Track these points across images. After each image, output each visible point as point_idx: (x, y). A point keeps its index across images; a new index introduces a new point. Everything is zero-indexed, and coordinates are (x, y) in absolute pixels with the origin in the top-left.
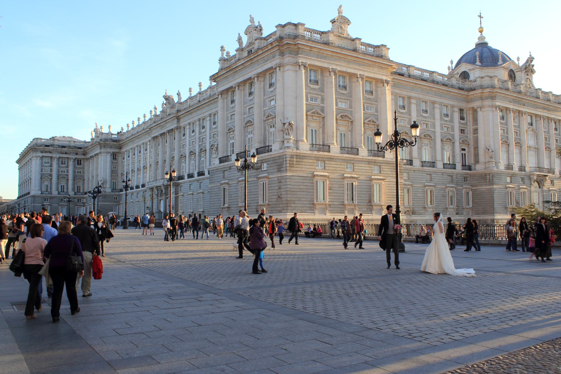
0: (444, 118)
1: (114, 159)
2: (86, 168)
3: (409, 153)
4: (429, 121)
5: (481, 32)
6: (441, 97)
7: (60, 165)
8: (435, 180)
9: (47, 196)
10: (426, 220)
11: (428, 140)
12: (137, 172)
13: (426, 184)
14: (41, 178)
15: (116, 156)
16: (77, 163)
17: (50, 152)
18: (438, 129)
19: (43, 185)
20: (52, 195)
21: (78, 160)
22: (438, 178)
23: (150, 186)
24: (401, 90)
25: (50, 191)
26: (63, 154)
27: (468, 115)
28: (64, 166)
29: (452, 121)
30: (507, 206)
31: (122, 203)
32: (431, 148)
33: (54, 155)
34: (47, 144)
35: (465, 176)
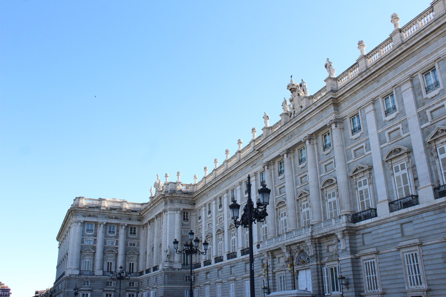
1: (184, 219)
2: (142, 238)
7: (108, 234)
9: (87, 278)
12: (228, 233)
14: (81, 252)
15: (187, 216)
16: (129, 232)
17: (94, 216)
19: (82, 261)
20: (94, 276)
21: (131, 228)
23: (273, 245)
25: (91, 270)
26: (112, 218)
28: (112, 235)
31: (199, 286)
33: (100, 221)
34: (92, 206)
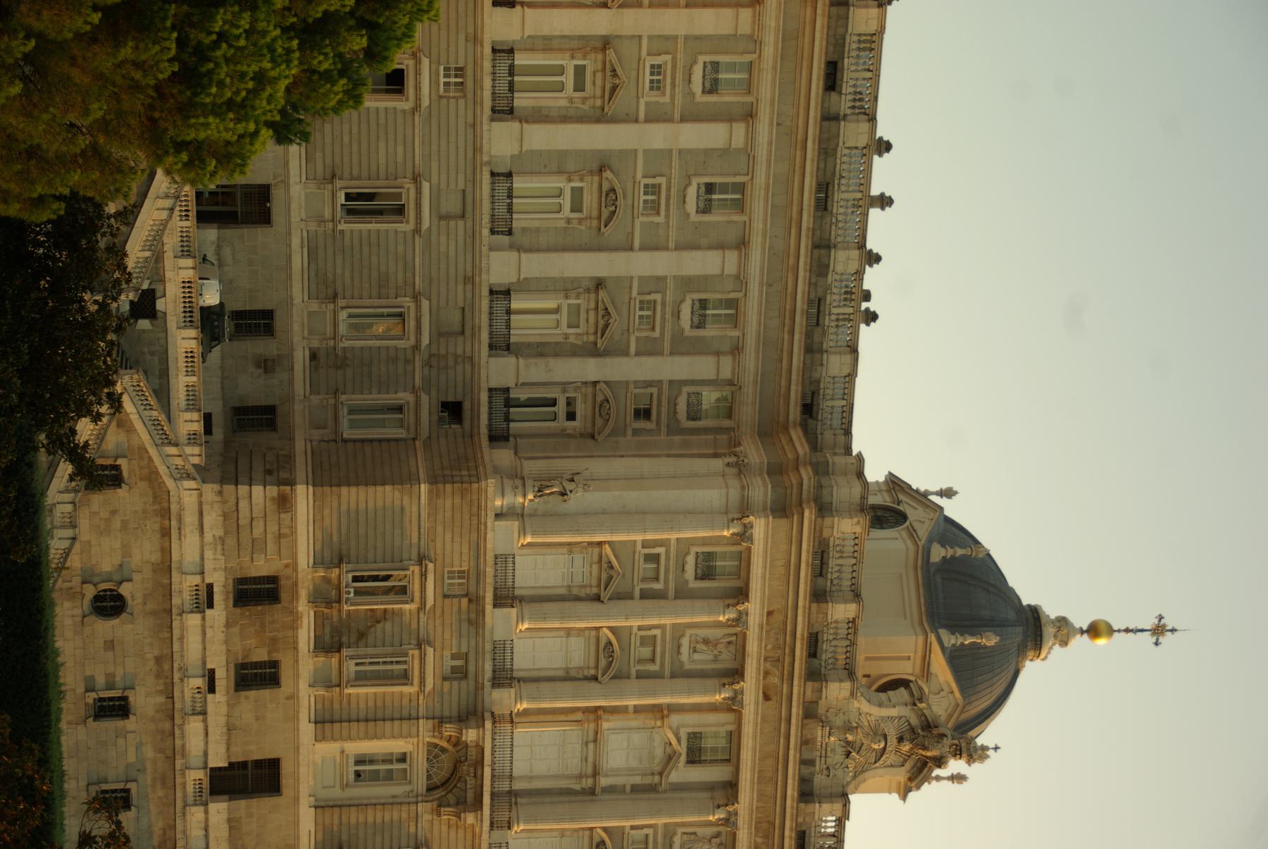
0: (688, 302)
3: (540, 109)
4: (667, 216)
5: (1094, 630)
6: (770, 285)
8: (443, 239)
10: (286, 183)
11: (595, 214)
13: (426, 186)
18: (641, 264)
22: (452, 253)
24: (775, 68)
27: (711, 437)
29: (682, 346)
30: (350, 566)
32: (562, 224)
35: (467, 406)
